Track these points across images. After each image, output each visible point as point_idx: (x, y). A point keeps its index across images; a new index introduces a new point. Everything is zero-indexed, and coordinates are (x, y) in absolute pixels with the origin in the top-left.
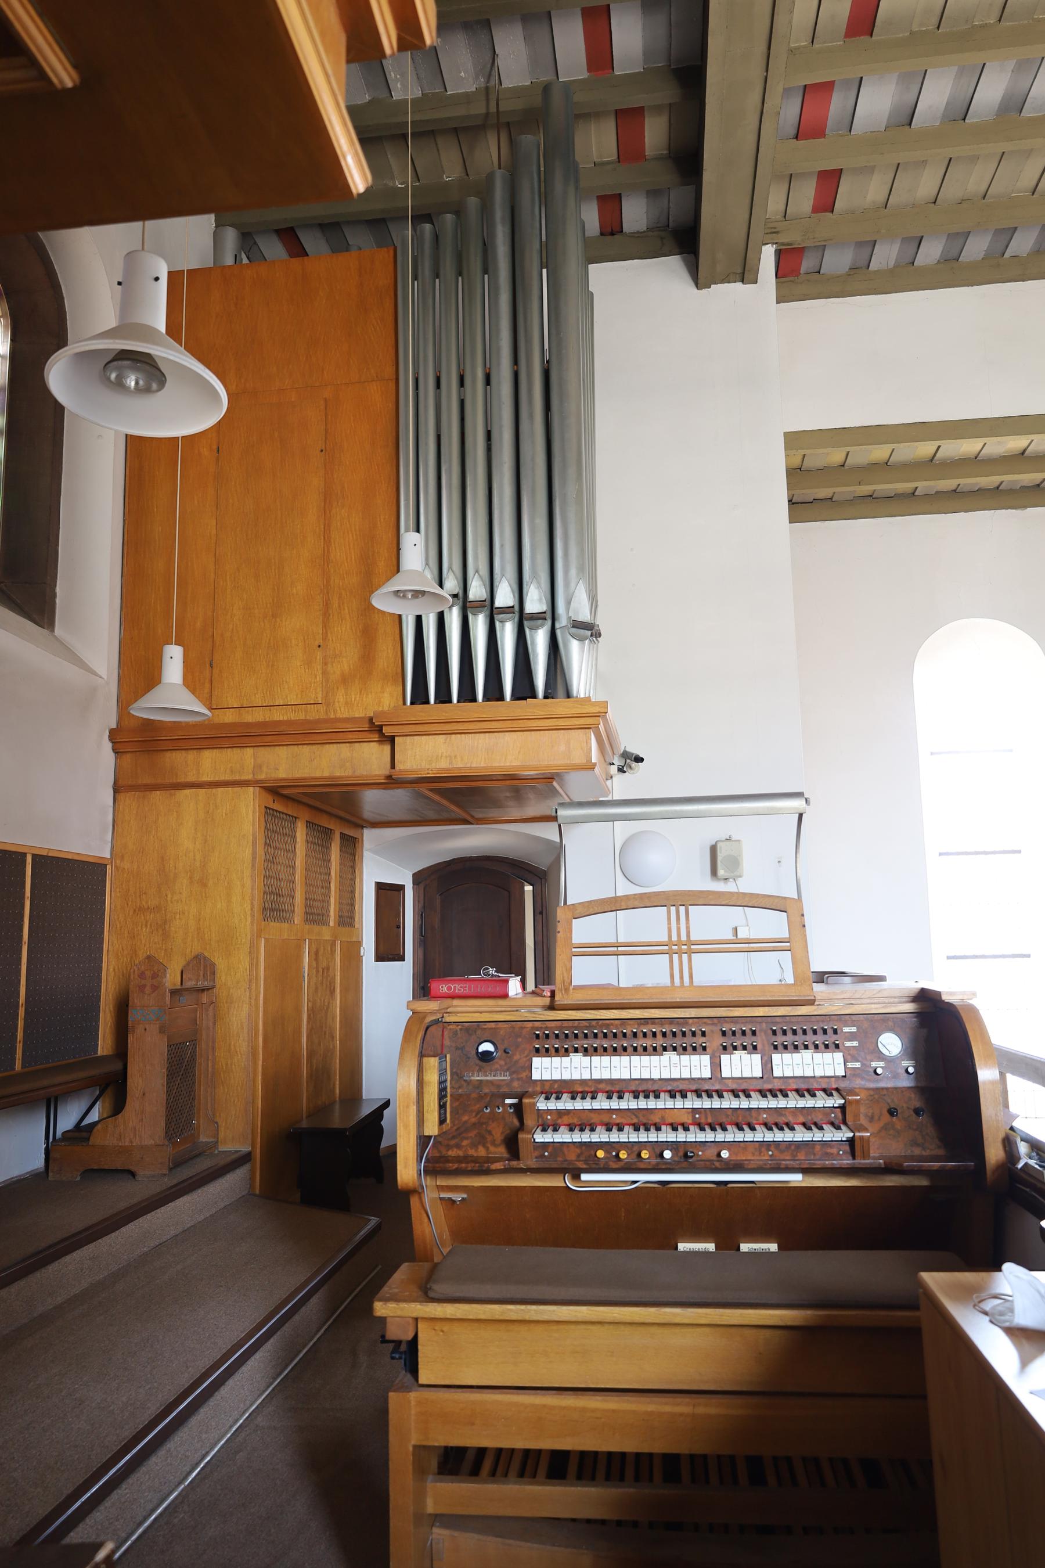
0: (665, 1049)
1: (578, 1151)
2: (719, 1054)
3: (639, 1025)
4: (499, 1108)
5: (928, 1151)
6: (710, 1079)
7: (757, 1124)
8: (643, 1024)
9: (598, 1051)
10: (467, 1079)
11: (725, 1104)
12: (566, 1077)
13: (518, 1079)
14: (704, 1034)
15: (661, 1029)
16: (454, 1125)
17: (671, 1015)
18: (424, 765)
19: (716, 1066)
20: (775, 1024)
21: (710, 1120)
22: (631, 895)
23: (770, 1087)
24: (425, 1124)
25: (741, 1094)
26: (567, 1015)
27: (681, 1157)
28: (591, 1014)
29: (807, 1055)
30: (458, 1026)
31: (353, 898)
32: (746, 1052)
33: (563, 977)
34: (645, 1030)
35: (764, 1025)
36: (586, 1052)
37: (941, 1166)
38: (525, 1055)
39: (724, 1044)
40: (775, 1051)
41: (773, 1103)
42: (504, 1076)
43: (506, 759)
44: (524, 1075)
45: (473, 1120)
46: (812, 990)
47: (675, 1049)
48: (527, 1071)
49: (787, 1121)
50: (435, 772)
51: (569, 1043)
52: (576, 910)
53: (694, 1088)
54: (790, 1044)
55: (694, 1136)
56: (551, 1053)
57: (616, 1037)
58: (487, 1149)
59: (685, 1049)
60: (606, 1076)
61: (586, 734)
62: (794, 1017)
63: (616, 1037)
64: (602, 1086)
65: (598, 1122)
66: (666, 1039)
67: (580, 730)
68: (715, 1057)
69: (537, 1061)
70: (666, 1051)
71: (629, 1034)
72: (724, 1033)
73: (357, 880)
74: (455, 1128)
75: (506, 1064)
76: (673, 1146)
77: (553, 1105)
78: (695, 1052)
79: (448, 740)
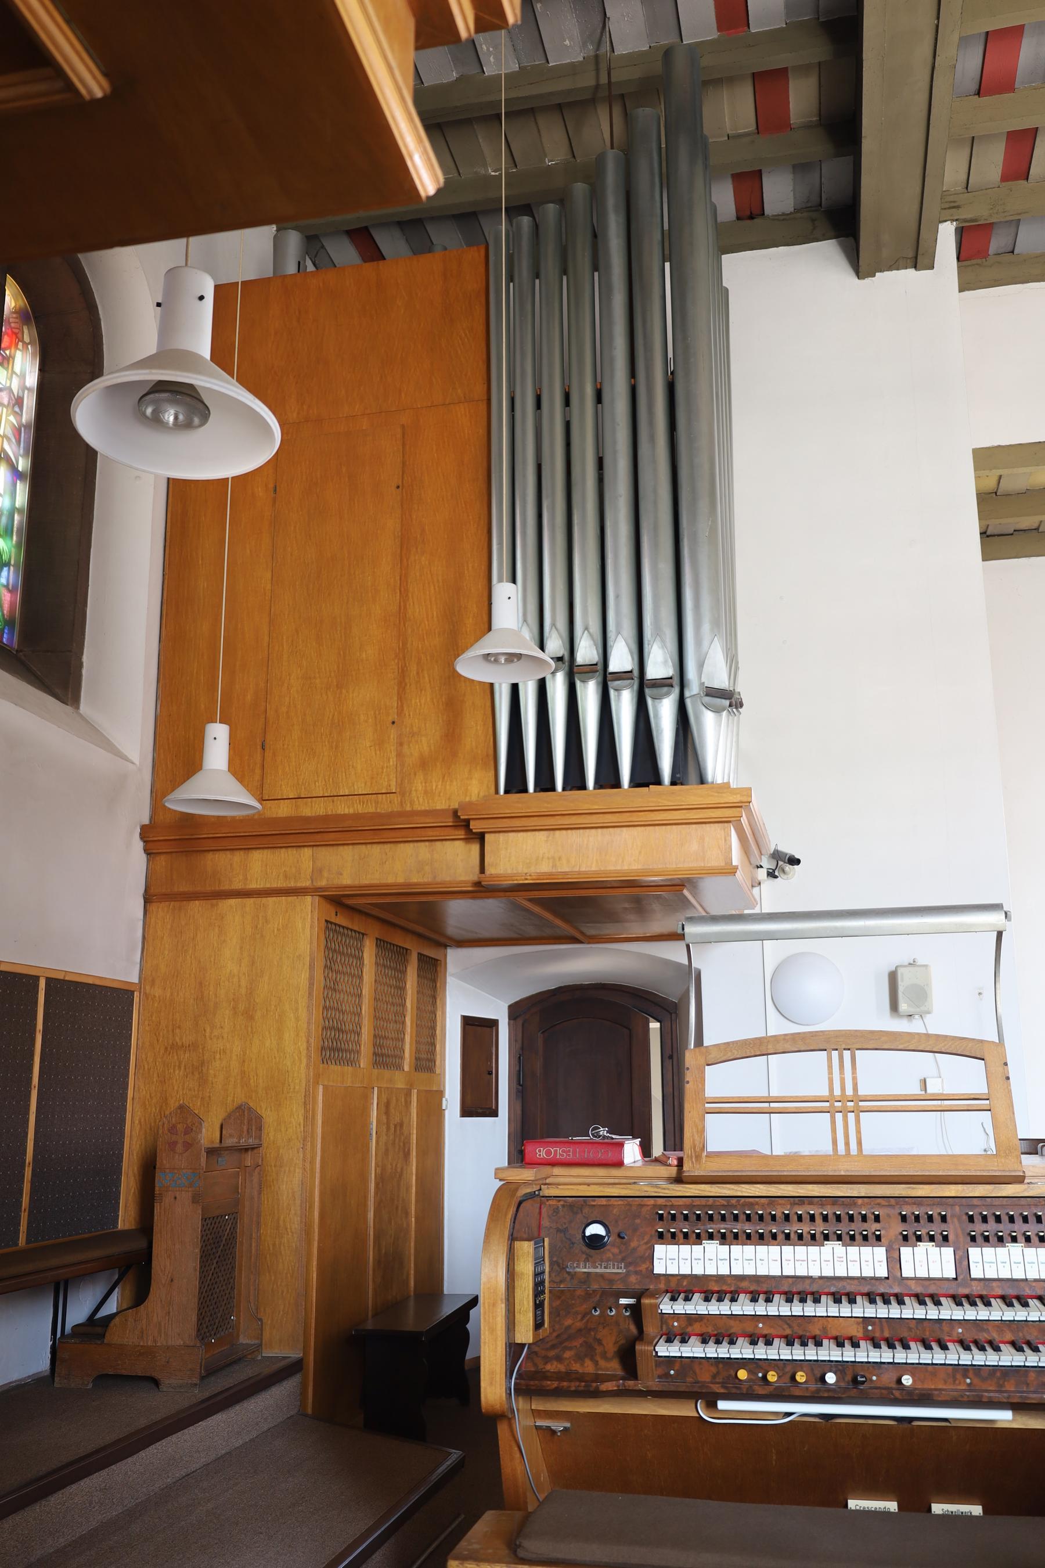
0: (826, 1238)
1: (714, 1370)
2: (897, 1247)
3: (793, 1204)
4: (611, 1311)
6: (887, 1278)
7: (950, 1341)
8: (797, 1204)
9: (740, 1238)
10: (571, 1271)
11: (907, 1313)
12: (698, 1271)
13: (636, 1273)
14: (877, 1219)
15: (821, 1211)
16: (554, 1331)
17: (834, 1192)
18: (521, 869)
19: (894, 1261)
20: (972, 1207)
21: (887, 1334)
22: (780, 1035)
23: (966, 1291)
24: (516, 1328)
25: (927, 1300)
26: (699, 1190)
27: (848, 1383)
28: (729, 1189)
29: (1015, 1250)
30: (560, 1201)
31: (433, 1036)
32: (934, 1244)
33: (694, 1140)
34: (800, 1212)
35: (957, 1208)
36: (723, 1239)
38: (645, 1241)
39: (905, 1233)
40: (973, 1243)
41: (970, 1314)
42: (618, 1268)
43: (623, 862)
44: (643, 1267)
45: (579, 1325)
46: (1021, 1163)
47: (839, 1238)
48: (648, 1263)
49: (989, 1338)
50: (534, 877)
51: (702, 1227)
52: (710, 1054)
53: (866, 1290)
54: (993, 1234)
55: (866, 1354)
56: (679, 1240)
57: (763, 1221)
58: (596, 1363)
59: (852, 1238)
60: (750, 1271)
61: (724, 830)
62: (997, 1199)
63: (763, 1221)
64: (744, 1285)
65: (740, 1332)
66: (827, 1224)
67: (716, 825)
68: (893, 1249)
69: (660, 1250)
70: (828, 1240)
71: (779, 1215)
72: (904, 1218)
73: (439, 1013)
74: (555, 1334)
75: (620, 1252)
76: (839, 1367)
77: (680, 1307)
78: (866, 1242)
79: (550, 838)
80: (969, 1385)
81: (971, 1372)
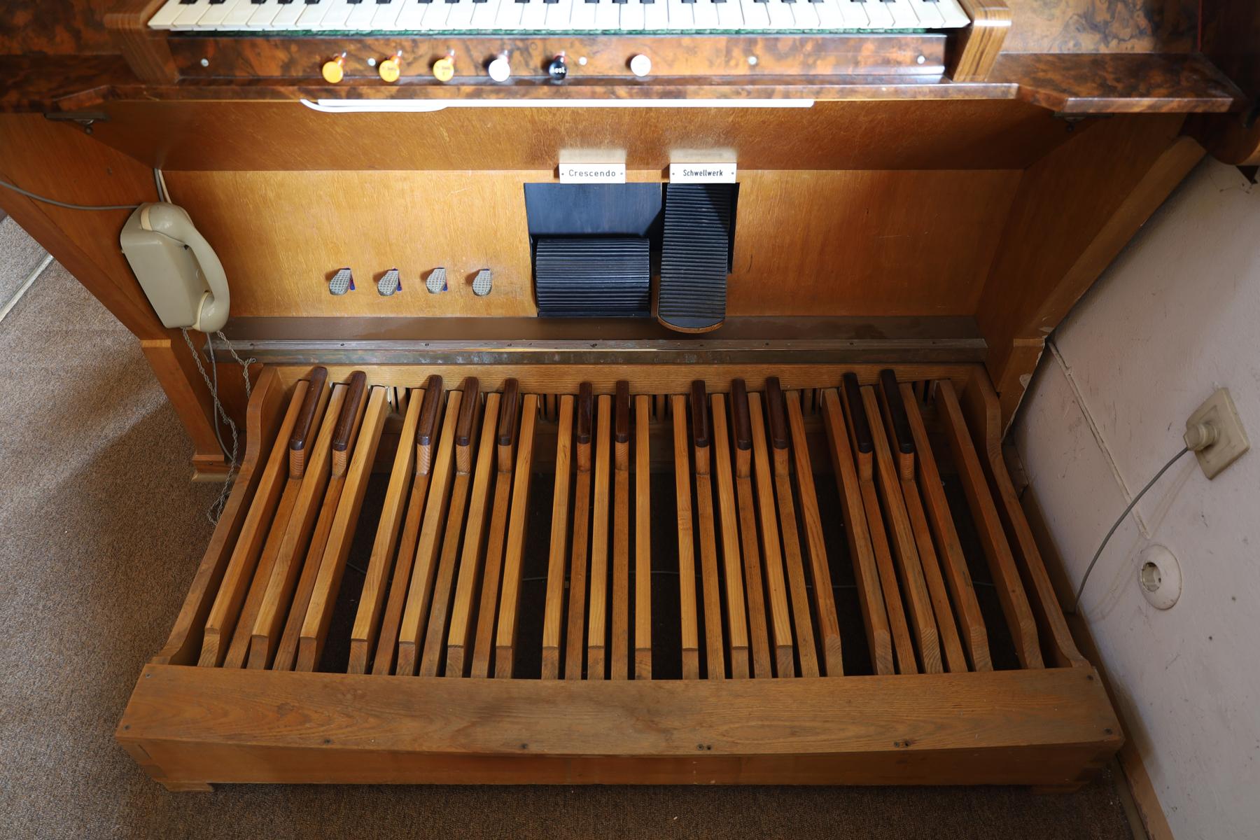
5: (1114, 43)
27: (535, 70)
37: (1150, 107)
58: (77, 35)
80: (753, 67)
81: (760, 45)
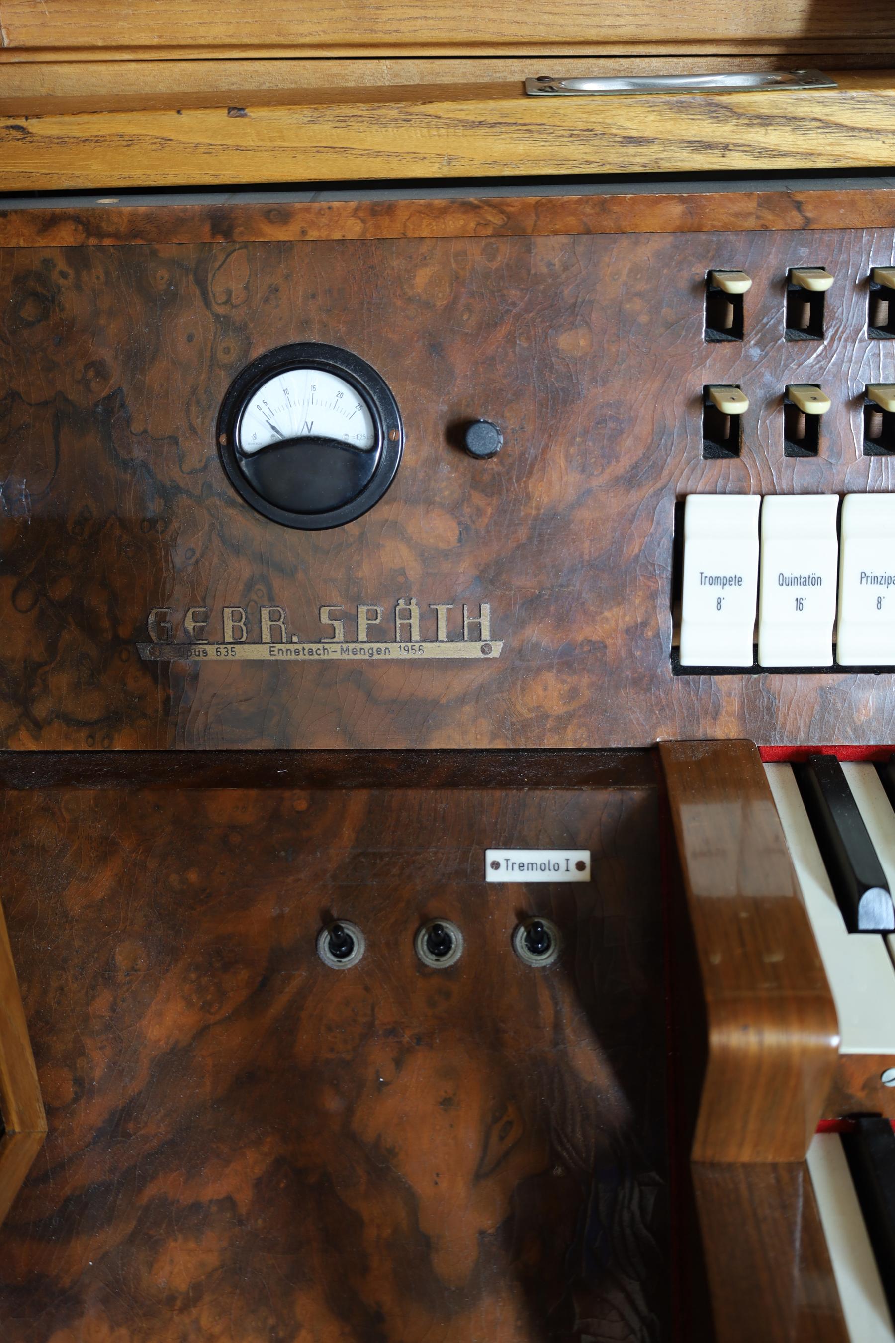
30: (51, 222)
38: (624, 464)
42: (455, 636)
